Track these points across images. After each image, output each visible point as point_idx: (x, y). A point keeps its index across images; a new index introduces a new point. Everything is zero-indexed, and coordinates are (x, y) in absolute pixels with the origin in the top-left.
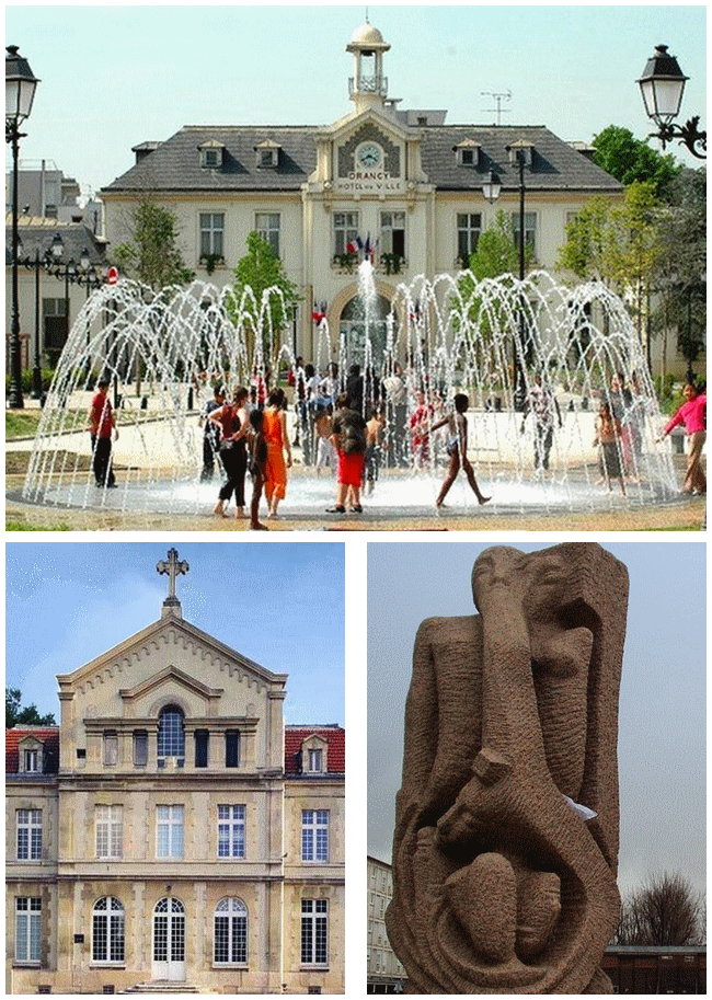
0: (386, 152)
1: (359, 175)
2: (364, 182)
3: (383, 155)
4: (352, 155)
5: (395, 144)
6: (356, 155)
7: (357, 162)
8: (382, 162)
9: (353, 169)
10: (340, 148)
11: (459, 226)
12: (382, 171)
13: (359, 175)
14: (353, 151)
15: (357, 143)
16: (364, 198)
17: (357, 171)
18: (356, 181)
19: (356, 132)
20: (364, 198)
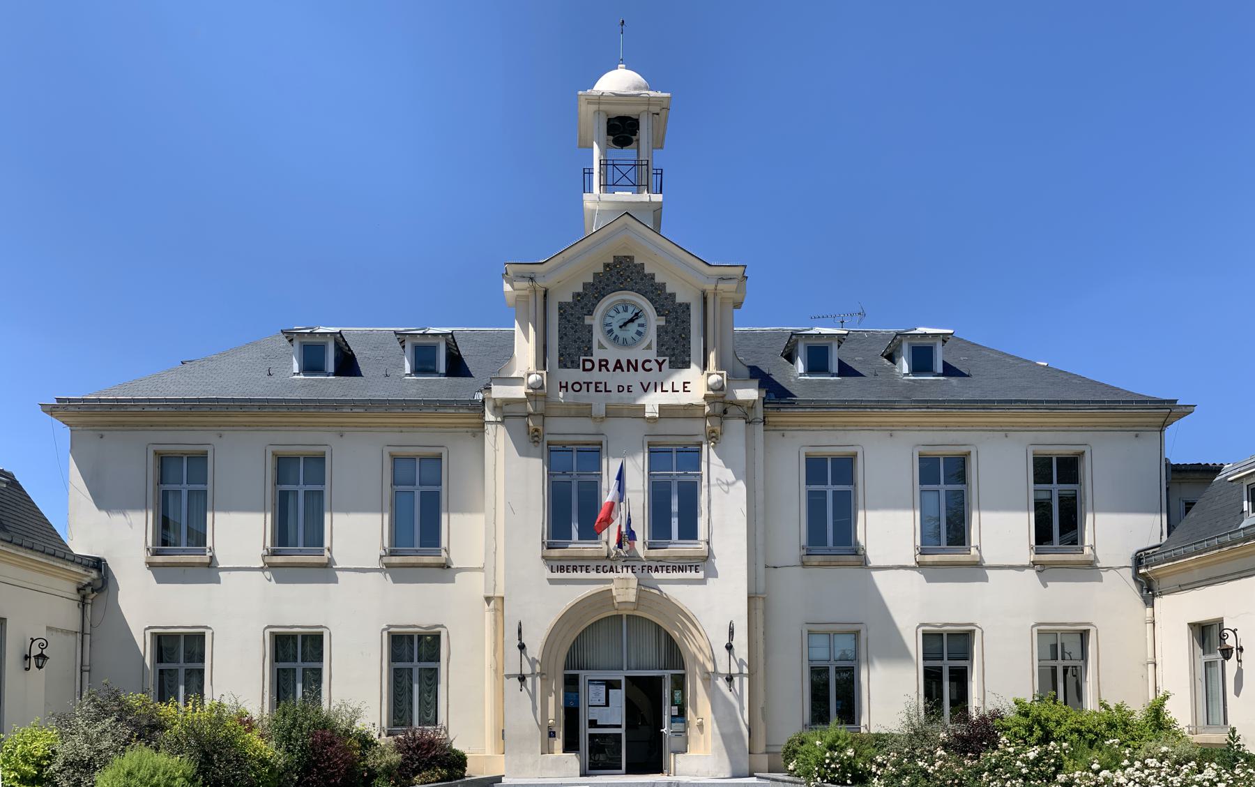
0: (659, 314)
1: (603, 364)
2: (614, 379)
3: (653, 321)
4: (588, 320)
5: (679, 299)
6: (595, 321)
7: (598, 336)
8: (652, 336)
9: (589, 351)
10: (562, 307)
11: (809, 481)
12: (652, 354)
13: (603, 364)
14: (590, 313)
15: (601, 295)
16: (612, 413)
17: (597, 355)
18: (596, 376)
19: (596, 275)
20: (612, 413)
